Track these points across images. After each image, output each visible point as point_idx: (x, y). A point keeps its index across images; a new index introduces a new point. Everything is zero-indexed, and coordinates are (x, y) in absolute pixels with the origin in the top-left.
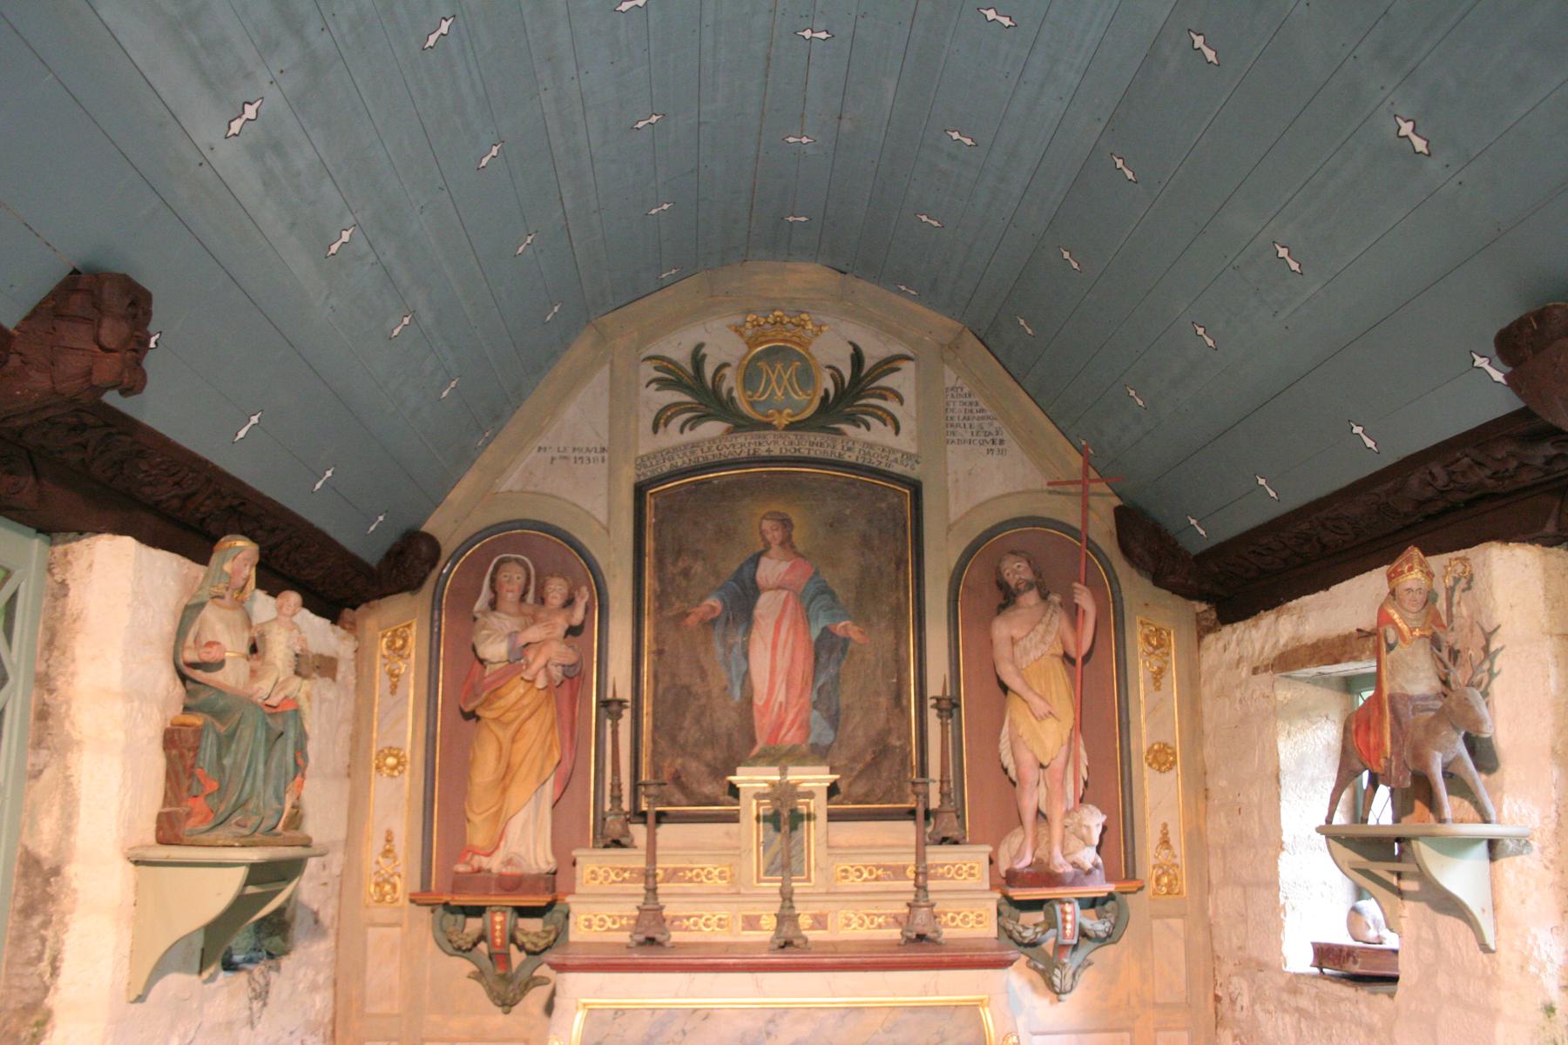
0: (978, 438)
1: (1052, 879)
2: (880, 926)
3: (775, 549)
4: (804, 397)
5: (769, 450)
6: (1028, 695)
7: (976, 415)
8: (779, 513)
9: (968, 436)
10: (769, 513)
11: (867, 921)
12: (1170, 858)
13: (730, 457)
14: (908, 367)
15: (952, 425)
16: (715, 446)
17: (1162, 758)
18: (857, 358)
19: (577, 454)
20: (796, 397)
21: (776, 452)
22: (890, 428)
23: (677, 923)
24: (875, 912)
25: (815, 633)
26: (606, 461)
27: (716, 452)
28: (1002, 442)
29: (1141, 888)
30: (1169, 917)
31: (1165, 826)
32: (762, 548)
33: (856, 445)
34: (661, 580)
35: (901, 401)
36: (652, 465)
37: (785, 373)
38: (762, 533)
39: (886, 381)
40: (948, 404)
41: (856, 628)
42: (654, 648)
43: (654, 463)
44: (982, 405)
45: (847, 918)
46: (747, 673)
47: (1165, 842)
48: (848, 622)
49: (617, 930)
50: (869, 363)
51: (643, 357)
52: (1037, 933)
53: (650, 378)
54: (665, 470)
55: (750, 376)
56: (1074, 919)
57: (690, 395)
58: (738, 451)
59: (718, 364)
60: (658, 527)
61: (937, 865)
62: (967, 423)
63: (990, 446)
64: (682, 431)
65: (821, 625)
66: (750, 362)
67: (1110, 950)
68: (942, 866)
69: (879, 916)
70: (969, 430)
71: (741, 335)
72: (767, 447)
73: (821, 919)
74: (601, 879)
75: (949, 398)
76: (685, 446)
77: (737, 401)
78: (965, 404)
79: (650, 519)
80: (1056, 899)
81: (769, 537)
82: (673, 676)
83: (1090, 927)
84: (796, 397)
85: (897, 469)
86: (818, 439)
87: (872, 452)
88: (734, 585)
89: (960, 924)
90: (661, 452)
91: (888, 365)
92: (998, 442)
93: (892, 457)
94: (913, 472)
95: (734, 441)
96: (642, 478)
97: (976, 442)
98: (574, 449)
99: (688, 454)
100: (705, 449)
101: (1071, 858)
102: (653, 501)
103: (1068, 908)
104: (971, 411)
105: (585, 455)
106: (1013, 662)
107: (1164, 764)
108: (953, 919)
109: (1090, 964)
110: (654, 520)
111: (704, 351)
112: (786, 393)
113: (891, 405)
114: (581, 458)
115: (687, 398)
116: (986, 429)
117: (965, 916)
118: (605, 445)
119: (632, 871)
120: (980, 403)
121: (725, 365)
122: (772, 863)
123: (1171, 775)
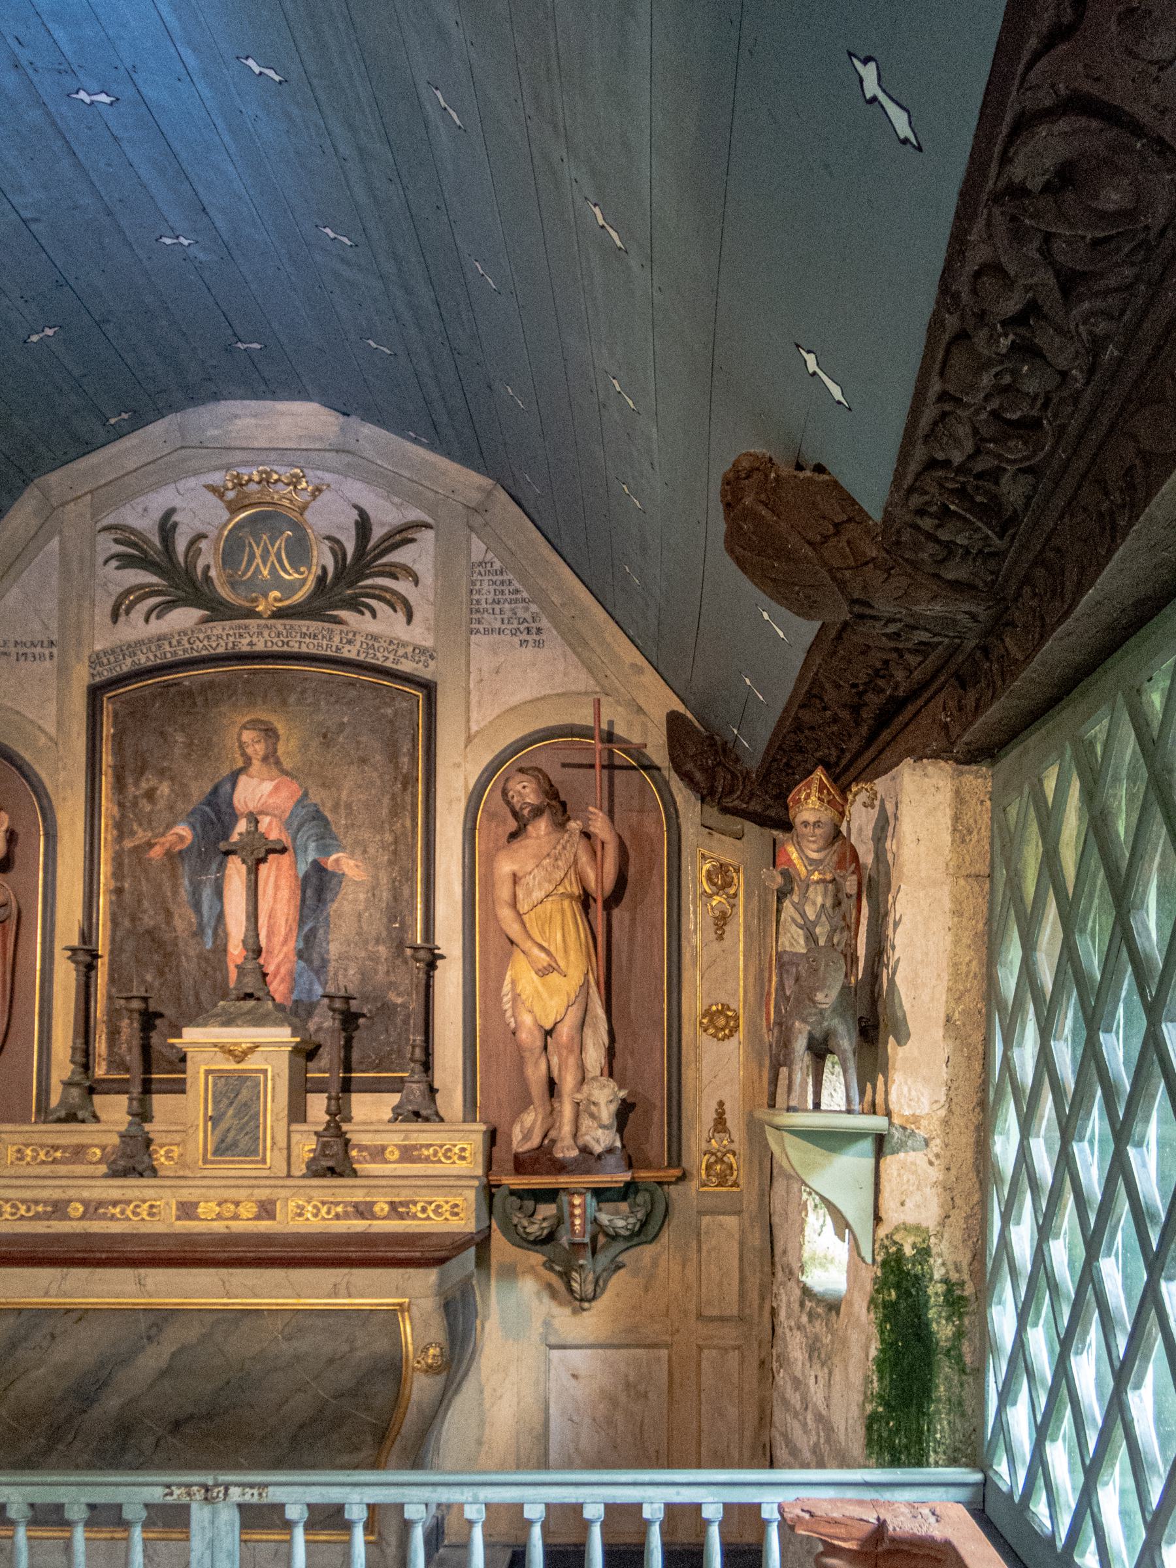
0: (510, 627)
1: (561, 1167)
2: (337, 1217)
3: (256, 764)
4: (296, 576)
5: (251, 644)
6: (528, 945)
7: (507, 596)
8: (262, 722)
9: (497, 625)
10: (252, 721)
11: (324, 1210)
12: (725, 1142)
13: (204, 653)
14: (427, 536)
15: (478, 611)
16: (186, 638)
17: (721, 1022)
18: (363, 526)
19: (21, 650)
20: (287, 577)
21: (260, 647)
22: (401, 616)
23: (101, 1211)
24: (332, 1199)
25: (303, 868)
26: (55, 659)
27: (187, 646)
28: (539, 630)
29: (683, 1178)
30: (719, 1213)
31: (721, 1104)
32: (240, 763)
33: (358, 636)
34: (121, 805)
35: (416, 582)
36: (109, 663)
37: (273, 546)
38: (242, 746)
39: (396, 557)
40: (473, 583)
41: (352, 863)
42: (112, 885)
43: (112, 659)
44: (517, 585)
45: (298, 1207)
46: (220, 917)
47: (720, 1123)
48: (341, 854)
49: (31, 1219)
50: (377, 533)
51: (99, 526)
52: (543, 1229)
53: (108, 555)
54: (125, 669)
55: (232, 551)
56: (585, 1212)
57: (155, 574)
58: (214, 645)
59: (193, 534)
60: (118, 739)
61: (422, 1146)
62: (497, 608)
63: (525, 636)
64: (147, 620)
65: (310, 859)
66: (230, 531)
67: (647, 1253)
68: (429, 1146)
69: (337, 1204)
70: (499, 617)
71: (221, 496)
72: (248, 640)
73: (269, 1207)
74: (28, 1159)
75: (475, 577)
76: (150, 641)
77: (216, 582)
78: (494, 583)
79: (108, 730)
80: (564, 1189)
81: (249, 751)
82: (133, 919)
83: (607, 1223)
84: (287, 577)
85: (406, 666)
86: (311, 630)
87: (376, 645)
88: (207, 809)
89: (432, 1215)
90: (121, 647)
91: (402, 536)
92: (534, 631)
93: (401, 652)
94: (425, 672)
95: (209, 632)
96: (98, 679)
97: (507, 632)
98: (16, 643)
99: (153, 649)
100: (174, 642)
101: (581, 1142)
102: (110, 707)
103: (577, 1201)
104: (502, 592)
105: (28, 651)
106: (514, 904)
107: (723, 1029)
108: (424, 1210)
109: (619, 1267)
110: (112, 731)
111: (175, 518)
112: (273, 570)
113: (402, 586)
114: (25, 654)
115: (154, 579)
116: (521, 614)
117: (439, 1206)
118: (54, 638)
119: (65, 1148)
120: (515, 582)
121: (201, 536)
122: (223, 1141)
123: (733, 1042)
